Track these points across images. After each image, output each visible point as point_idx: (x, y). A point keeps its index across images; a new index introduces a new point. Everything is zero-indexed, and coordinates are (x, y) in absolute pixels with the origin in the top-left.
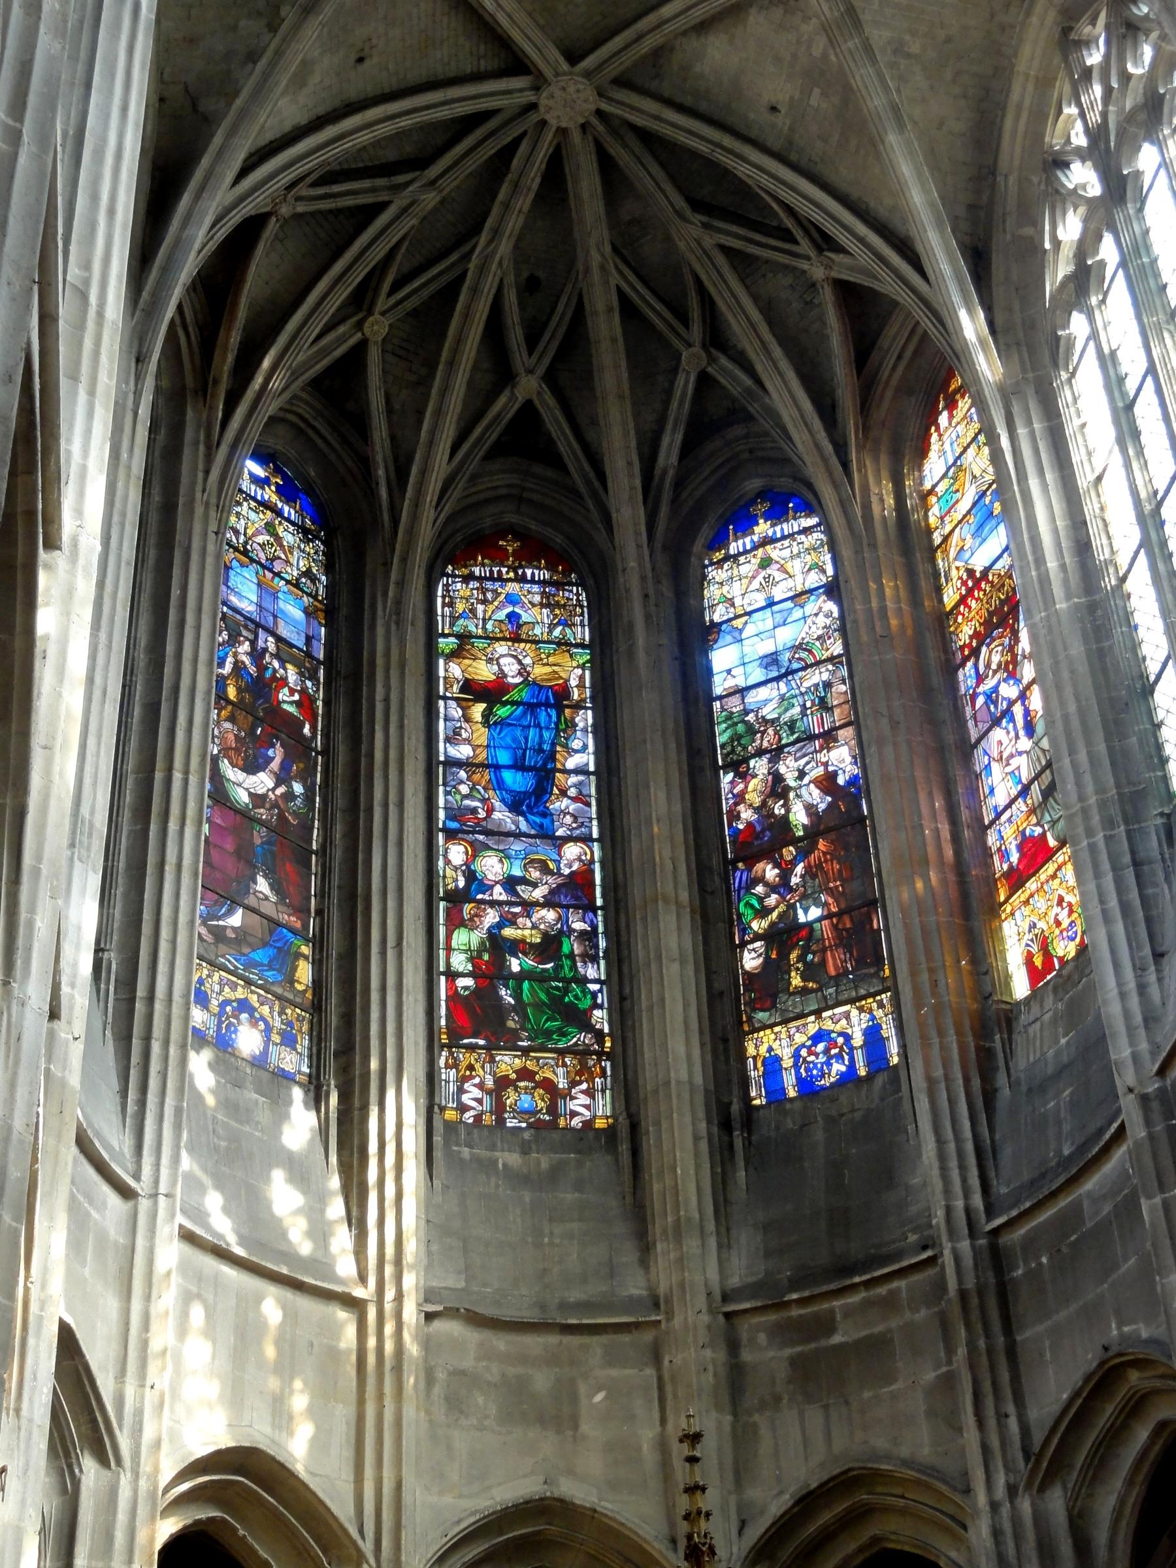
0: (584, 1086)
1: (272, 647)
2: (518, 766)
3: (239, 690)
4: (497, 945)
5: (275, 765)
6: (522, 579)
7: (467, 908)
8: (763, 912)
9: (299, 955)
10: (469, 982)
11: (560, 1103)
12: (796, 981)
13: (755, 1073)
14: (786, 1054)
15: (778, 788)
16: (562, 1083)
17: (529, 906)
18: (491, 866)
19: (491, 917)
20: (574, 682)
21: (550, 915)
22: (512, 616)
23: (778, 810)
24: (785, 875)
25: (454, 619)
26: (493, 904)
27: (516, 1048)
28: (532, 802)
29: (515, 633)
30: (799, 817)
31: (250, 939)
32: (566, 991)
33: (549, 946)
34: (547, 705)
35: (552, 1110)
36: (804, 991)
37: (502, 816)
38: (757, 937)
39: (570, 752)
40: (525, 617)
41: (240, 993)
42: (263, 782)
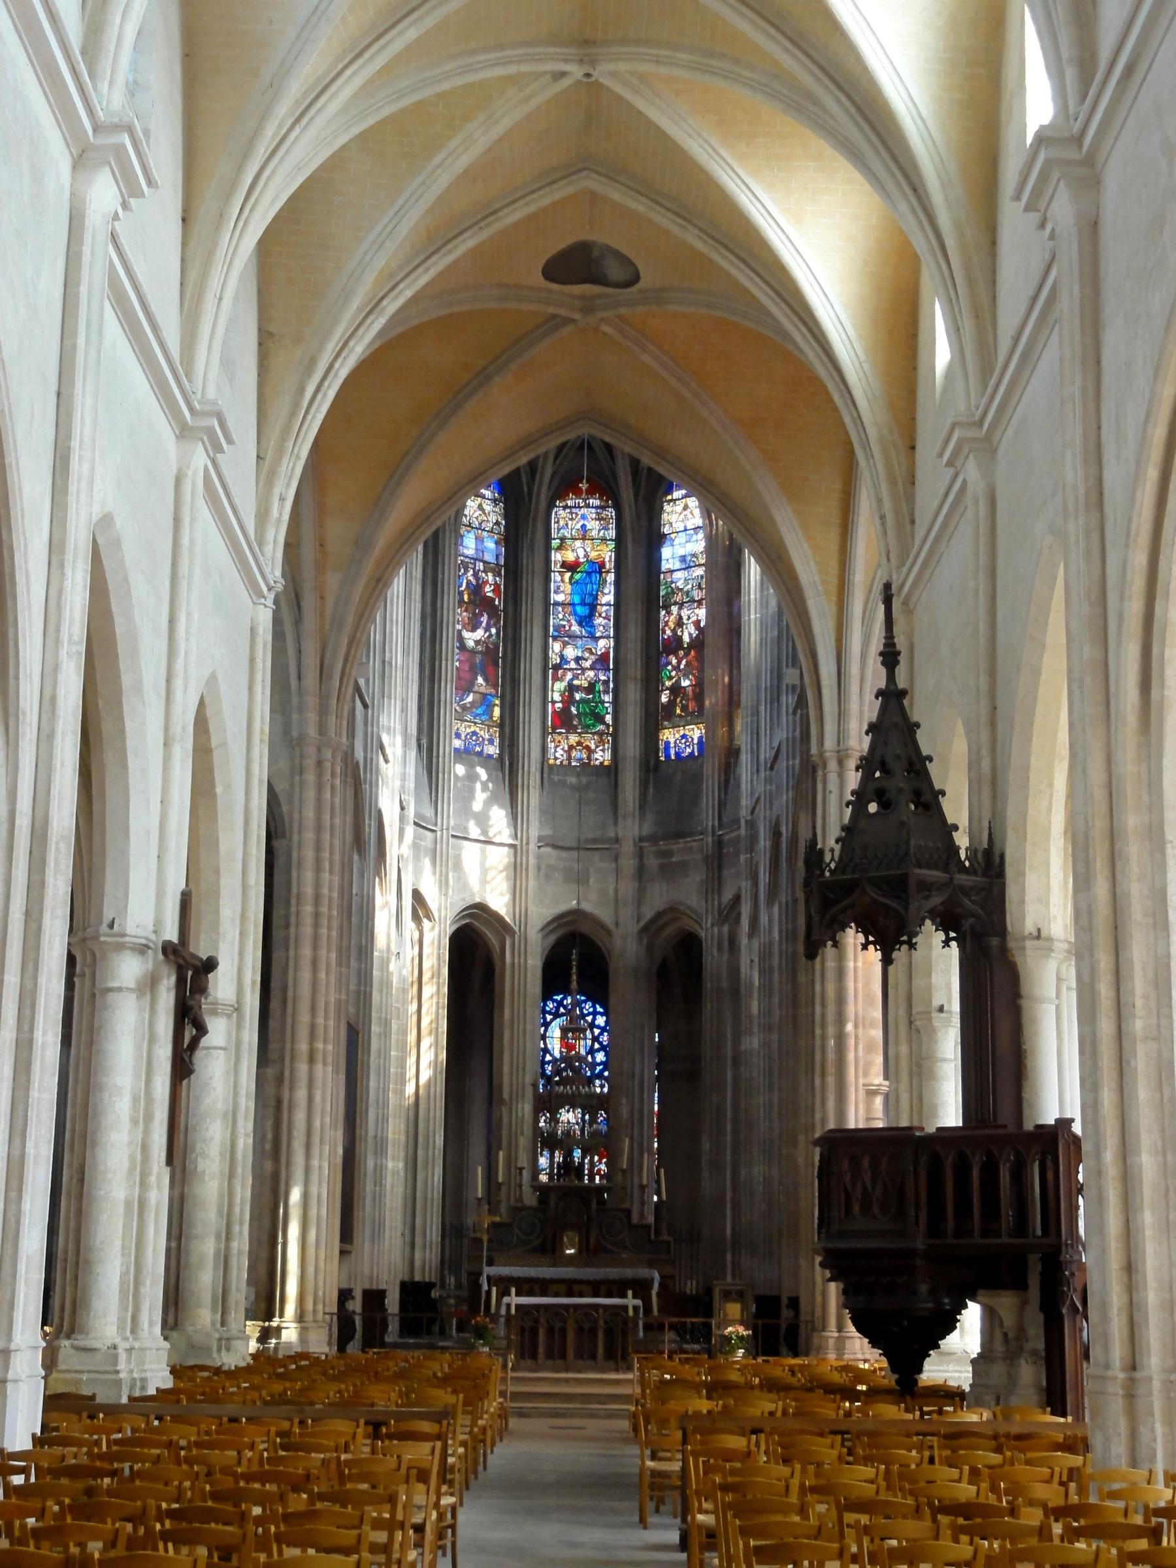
1: (482, 568)
2: (583, 603)
4: (571, 688)
5: (484, 625)
6: (588, 506)
7: (560, 672)
8: (670, 678)
10: (560, 705)
12: (678, 711)
13: (662, 747)
14: (672, 740)
15: (680, 623)
16: (593, 747)
17: (584, 670)
18: (570, 653)
19: (569, 676)
20: (607, 559)
22: (584, 526)
23: (679, 633)
24: (679, 663)
25: (559, 530)
26: (570, 670)
28: (586, 621)
29: (584, 535)
30: (686, 639)
32: (596, 707)
35: (589, 758)
36: (680, 716)
37: (575, 628)
38: (667, 689)
40: (589, 527)
41: (472, 729)
42: (479, 634)
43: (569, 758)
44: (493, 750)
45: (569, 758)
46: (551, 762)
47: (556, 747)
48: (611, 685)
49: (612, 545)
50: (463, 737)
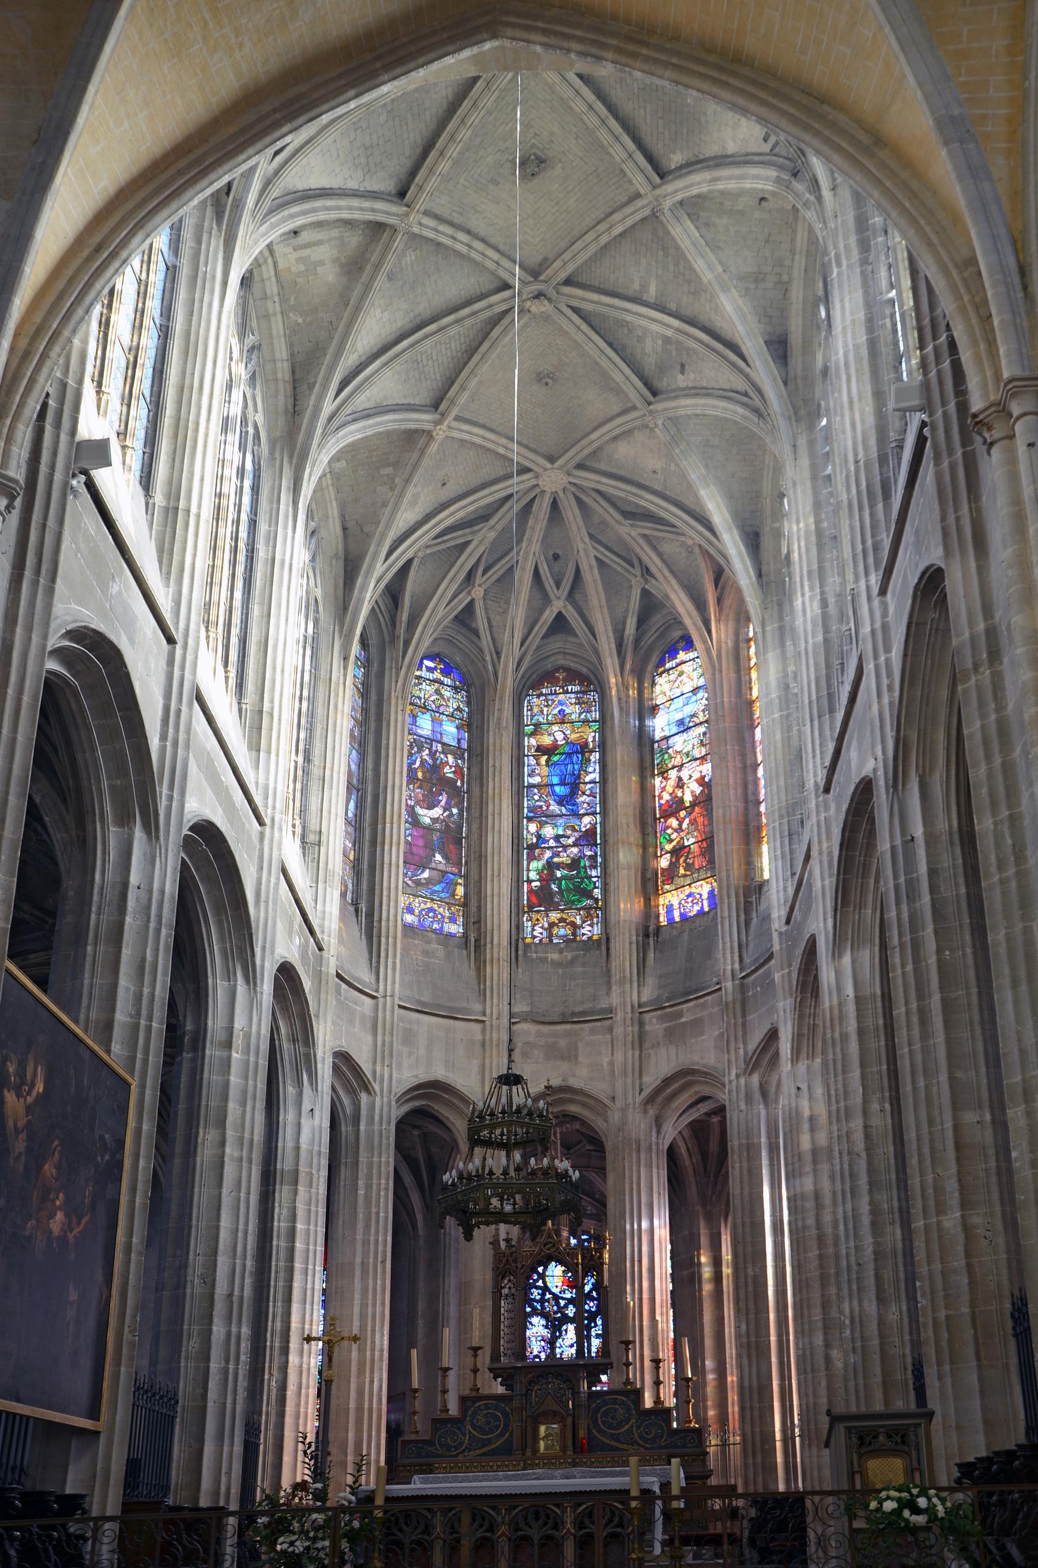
1: (440, 748)
2: (562, 783)
3: (424, 773)
4: (550, 866)
5: (443, 803)
9: (457, 884)
10: (538, 884)
16: (579, 922)
17: (565, 847)
18: (548, 831)
19: (548, 854)
20: (590, 740)
21: (575, 850)
22: (561, 711)
25: (532, 716)
29: (562, 719)
33: (575, 864)
34: (577, 752)
35: (574, 934)
37: (554, 808)
39: (587, 773)
41: (429, 905)
42: (437, 812)
44: (456, 929)
45: (550, 936)
46: (528, 941)
49: (595, 726)
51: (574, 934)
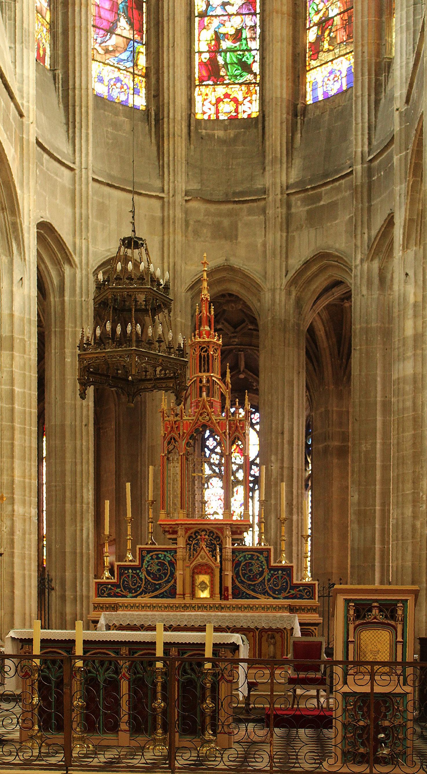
0: (249, 99)
4: (218, 37)
7: (206, 19)
11: (240, 107)
16: (240, 99)
21: (238, 19)
26: (216, 16)
27: (223, 84)
31: (119, 49)
35: (236, 111)
43: (217, 112)
44: (140, 101)
45: (217, 112)
46: (199, 116)
47: (205, 100)
48: (258, 31)
50: (106, 83)
51: (236, 111)
